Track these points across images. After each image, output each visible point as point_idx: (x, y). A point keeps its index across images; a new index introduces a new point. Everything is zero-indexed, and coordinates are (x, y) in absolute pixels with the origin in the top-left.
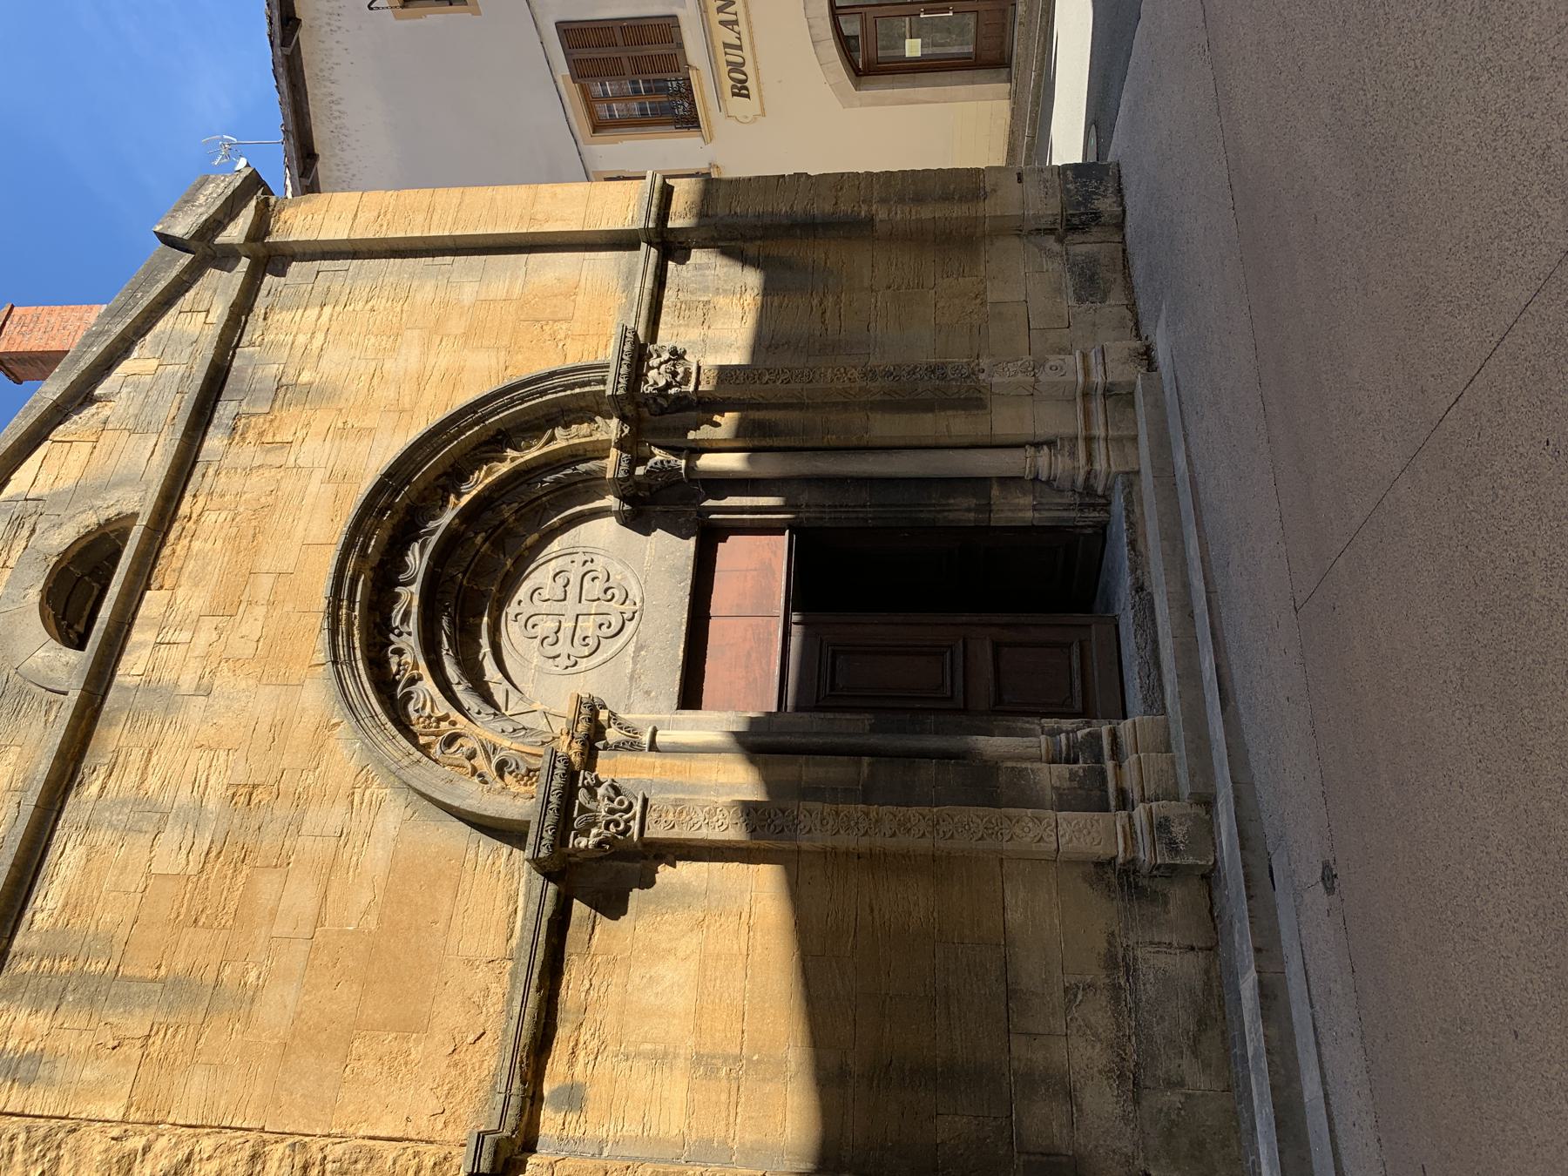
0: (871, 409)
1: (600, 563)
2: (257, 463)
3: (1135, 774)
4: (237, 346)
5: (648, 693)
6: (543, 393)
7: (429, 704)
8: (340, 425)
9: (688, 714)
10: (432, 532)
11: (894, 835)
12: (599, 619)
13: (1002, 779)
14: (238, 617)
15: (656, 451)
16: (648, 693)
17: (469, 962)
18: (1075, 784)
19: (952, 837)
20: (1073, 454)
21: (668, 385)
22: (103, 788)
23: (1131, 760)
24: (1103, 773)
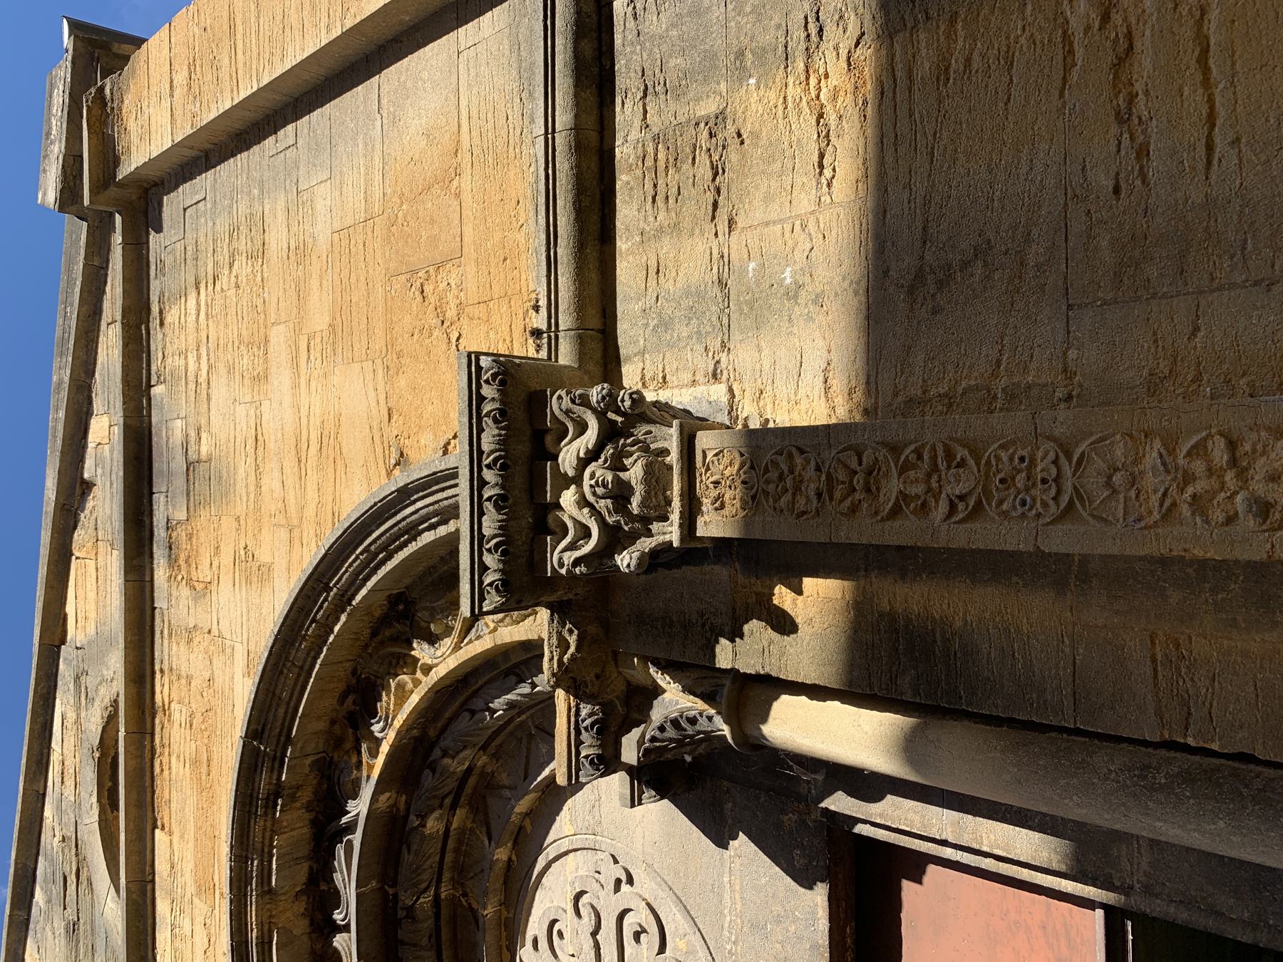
1: (645, 884)
4: (150, 386)
6: (413, 532)
10: (351, 828)
15: (662, 680)
21: (614, 539)
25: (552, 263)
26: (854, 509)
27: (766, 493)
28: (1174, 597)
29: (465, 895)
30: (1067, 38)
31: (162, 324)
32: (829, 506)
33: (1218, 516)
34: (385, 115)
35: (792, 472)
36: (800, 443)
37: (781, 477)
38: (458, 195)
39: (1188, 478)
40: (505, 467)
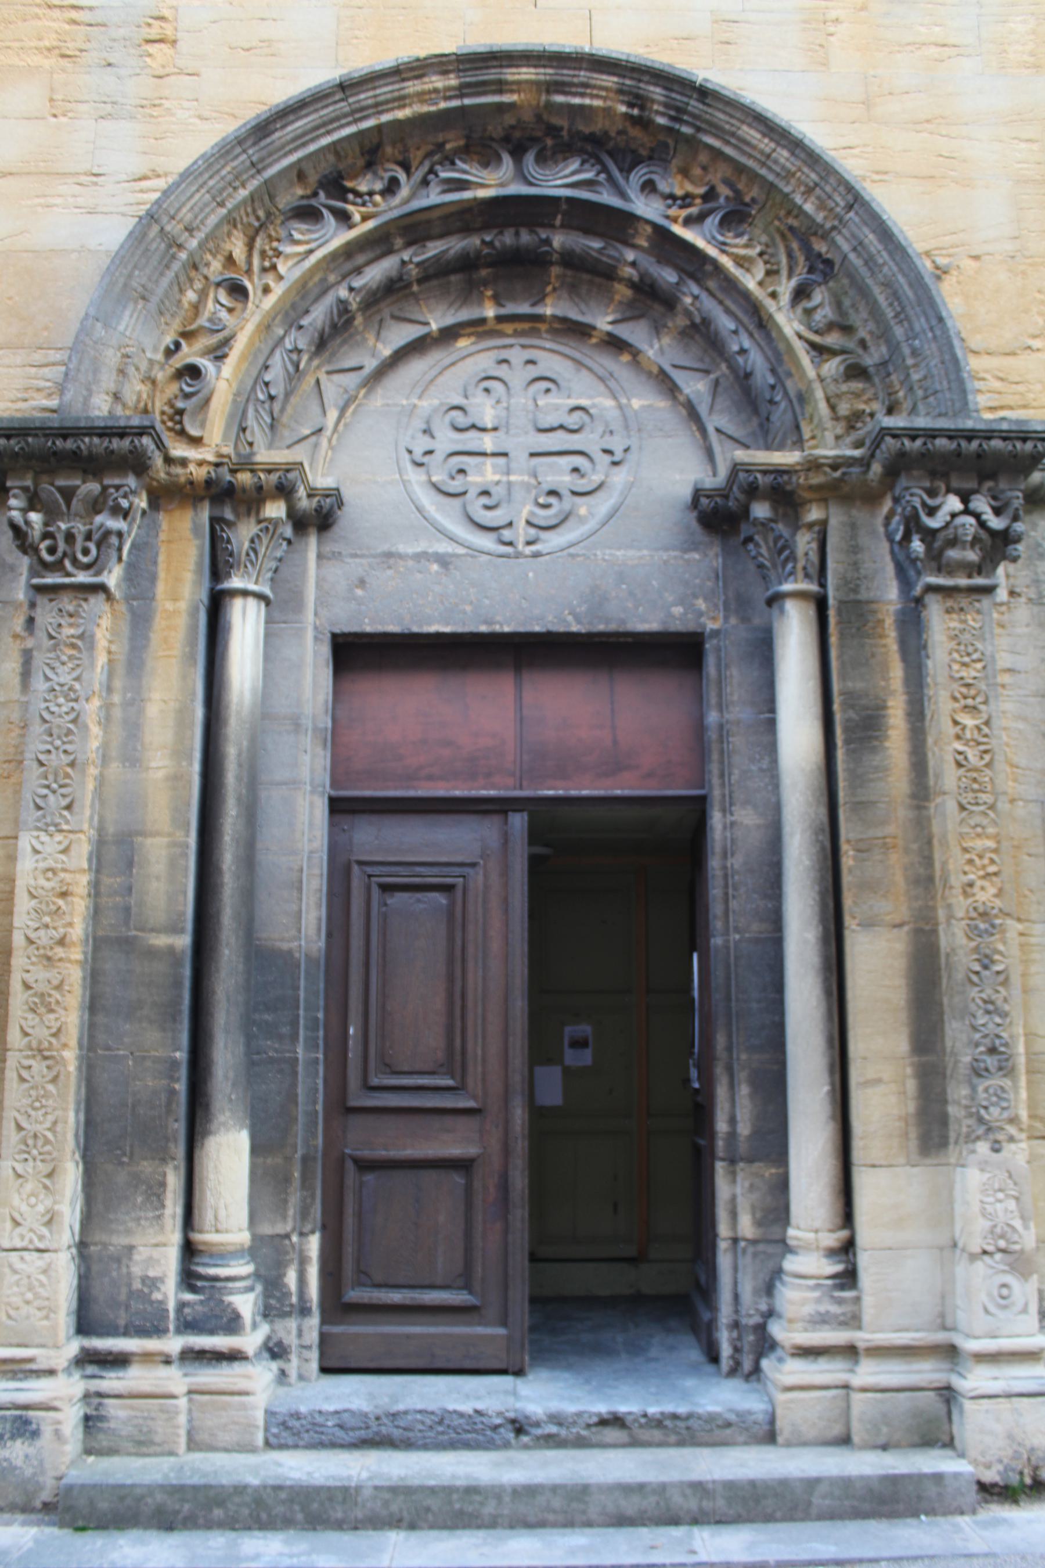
0: (918, 932)
3: (146, 1387)
5: (362, 583)
7: (301, 249)
9: (326, 650)
11: (27, 986)
12: (498, 492)
13: (146, 1167)
16: (362, 583)
18: (137, 1285)
19: (22, 1080)
20: (822, 1320)
23: (175, 1380)
24: (158, 1330)
26: (955, 699)
27: (959, 644)
28: (915, 847)
29: (554, 289)
32: (955, 686)
33: (967, 868)
35: (974, 661)
36: (989, 667)
37: (969, 655)
39: (981, 857)
40: (980, 455)
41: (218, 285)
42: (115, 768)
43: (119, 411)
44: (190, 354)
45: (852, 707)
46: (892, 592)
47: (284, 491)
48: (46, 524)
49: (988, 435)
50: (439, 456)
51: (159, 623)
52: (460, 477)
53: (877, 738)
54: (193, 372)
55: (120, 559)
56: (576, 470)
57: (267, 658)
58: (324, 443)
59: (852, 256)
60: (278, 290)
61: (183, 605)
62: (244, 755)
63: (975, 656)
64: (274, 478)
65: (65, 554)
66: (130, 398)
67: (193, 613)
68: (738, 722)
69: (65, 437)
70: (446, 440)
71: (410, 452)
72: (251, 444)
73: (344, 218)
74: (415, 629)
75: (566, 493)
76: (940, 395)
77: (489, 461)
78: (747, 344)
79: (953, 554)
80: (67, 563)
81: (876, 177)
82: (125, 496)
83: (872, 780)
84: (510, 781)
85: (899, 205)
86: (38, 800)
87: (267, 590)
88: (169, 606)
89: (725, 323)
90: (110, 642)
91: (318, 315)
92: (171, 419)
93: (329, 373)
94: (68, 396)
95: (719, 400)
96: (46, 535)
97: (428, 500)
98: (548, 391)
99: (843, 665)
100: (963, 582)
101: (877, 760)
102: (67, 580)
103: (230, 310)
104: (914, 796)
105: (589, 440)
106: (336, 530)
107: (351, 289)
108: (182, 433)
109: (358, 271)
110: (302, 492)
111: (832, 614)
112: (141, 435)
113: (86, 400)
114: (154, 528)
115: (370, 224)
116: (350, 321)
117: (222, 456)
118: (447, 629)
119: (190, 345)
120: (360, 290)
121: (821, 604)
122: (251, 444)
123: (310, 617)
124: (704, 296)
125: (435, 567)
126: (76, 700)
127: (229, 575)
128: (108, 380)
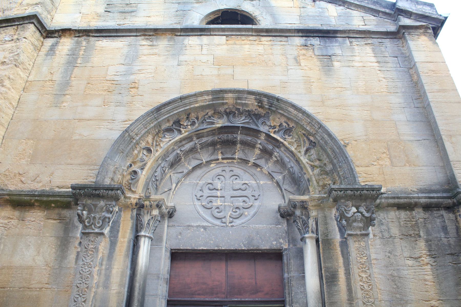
2: (288, 56)
5: (180, 233)
7: (167, 140)
8: (312, 80)
9: (168, 254)
12: (222, 208)
14: (213, 66)
17: (52, 174)
22: (144, 45)
25: (394, 198)
26: (359, 268)
27: (359, 251)
30: (429, 301)
31: (366, 44)
34: (422, 141)
37: (362, 255)
38: (405, 165)
41: (144, 149)
42: (101, 289)
43: (112, 183)
44: (134, 168)
45: (328, 272)
46: (337, 237)
47: (159, 206)
48: (88, 214)
49: (363, 189)
50: (204, 197)
51: (119, 244)
52: (210, 203)
53: (336, 281)
54: (135, 172)
55: (109, 225)
56: (244, 201)
57: (150, 256)
58: (171, 193)
59: (321, 141)
60: (160, 151)
61: (126, 240)
62: (141, 286)
63: (364, 255)
64: (156, 203)
65: (92, 223)
66: (116, 179)
67: (129, 242)
68: (294, 277)
69: (96, 190)
70: (207, 192)
71: (196, 196)
72: (150, 193)
73: (180, 132)
74: (196, 248)
75: (241, 208)
76: (348, 179)
77: (219, 199)
78: (293, 165)
79: (355, 224)
80: (93, 226)
81: (326, 120)
82: (112, 207)
83: (335, 295)
84: (223, 296)
85: (333, 127)
86: (75, 299)
87: (152, 236)
88: (122, 240)
89: (286, 160)
90: (104, 250)
91: (171, 158)
92: (127, 186)
93: (173, 173)
94: (98, 178)
95: (285, 181)
96: (87, 218)
97: (201, 210)
98: (236, 179)
99: (324, 259)
100: (359, 233)
101: (336, 288)
102: (92, 231)
103: (147, 156)
104: (348, 300)
105: (248, 193)
106: (173, 218)
107: (181, 151)
108: (130, 189)
109: (183, 146)
110: (164, 207)
111: (320, 243)
112: (118, 190)
113: (103, 179)
114: (120, 216)
115: (187, 133)
116: (180, 160)
117: (141, 196)
118: (205, 249)
119: (134, 165)
120: (183, 151)
121: (317, 241)
122: (150, 193)
123: (164, 243)
124: (280, 152)
125: (202, 230)
126: (91, 268)
127: (141, 231)
128: (110, 175)
